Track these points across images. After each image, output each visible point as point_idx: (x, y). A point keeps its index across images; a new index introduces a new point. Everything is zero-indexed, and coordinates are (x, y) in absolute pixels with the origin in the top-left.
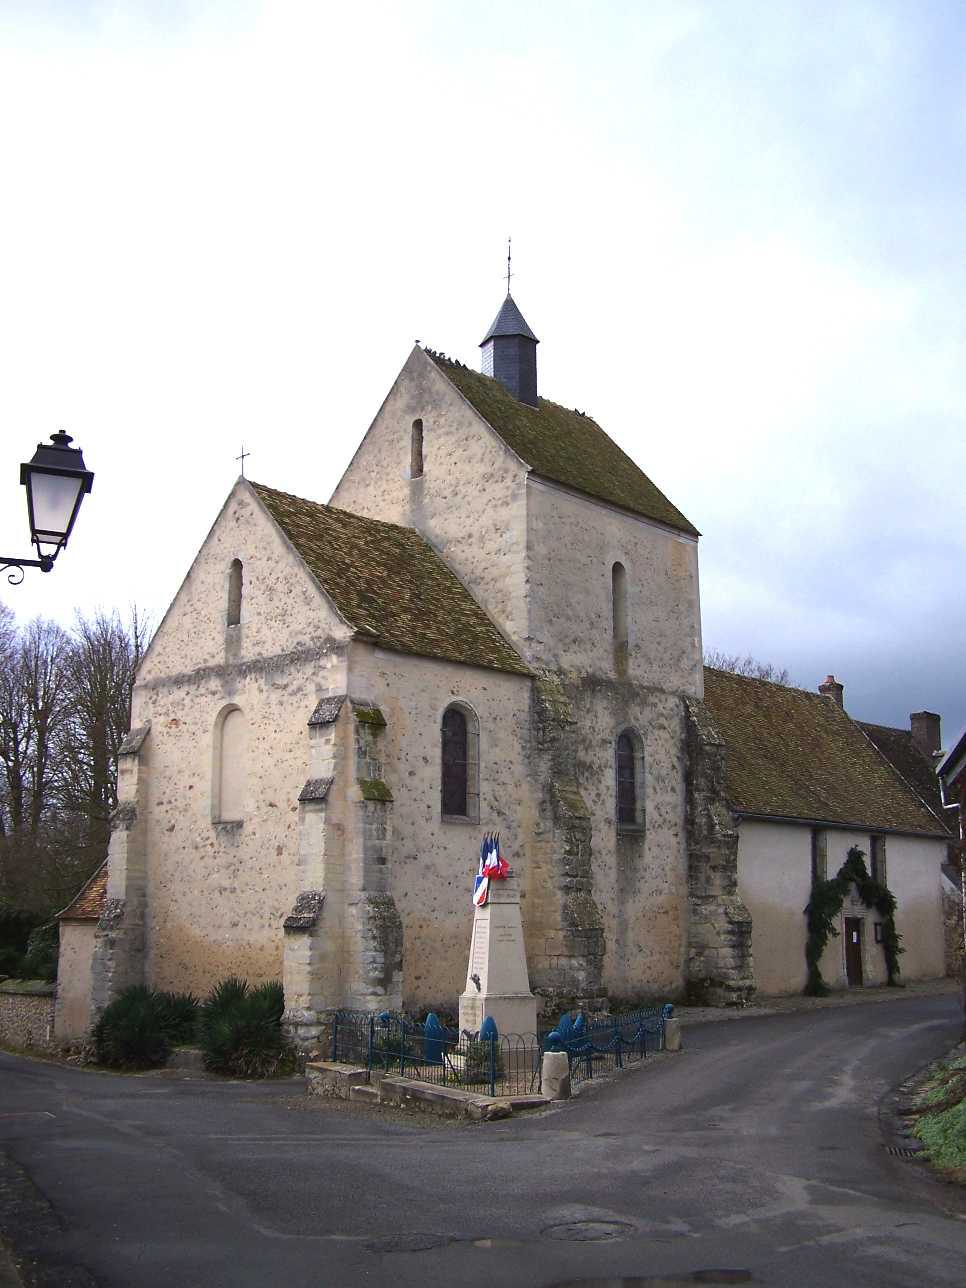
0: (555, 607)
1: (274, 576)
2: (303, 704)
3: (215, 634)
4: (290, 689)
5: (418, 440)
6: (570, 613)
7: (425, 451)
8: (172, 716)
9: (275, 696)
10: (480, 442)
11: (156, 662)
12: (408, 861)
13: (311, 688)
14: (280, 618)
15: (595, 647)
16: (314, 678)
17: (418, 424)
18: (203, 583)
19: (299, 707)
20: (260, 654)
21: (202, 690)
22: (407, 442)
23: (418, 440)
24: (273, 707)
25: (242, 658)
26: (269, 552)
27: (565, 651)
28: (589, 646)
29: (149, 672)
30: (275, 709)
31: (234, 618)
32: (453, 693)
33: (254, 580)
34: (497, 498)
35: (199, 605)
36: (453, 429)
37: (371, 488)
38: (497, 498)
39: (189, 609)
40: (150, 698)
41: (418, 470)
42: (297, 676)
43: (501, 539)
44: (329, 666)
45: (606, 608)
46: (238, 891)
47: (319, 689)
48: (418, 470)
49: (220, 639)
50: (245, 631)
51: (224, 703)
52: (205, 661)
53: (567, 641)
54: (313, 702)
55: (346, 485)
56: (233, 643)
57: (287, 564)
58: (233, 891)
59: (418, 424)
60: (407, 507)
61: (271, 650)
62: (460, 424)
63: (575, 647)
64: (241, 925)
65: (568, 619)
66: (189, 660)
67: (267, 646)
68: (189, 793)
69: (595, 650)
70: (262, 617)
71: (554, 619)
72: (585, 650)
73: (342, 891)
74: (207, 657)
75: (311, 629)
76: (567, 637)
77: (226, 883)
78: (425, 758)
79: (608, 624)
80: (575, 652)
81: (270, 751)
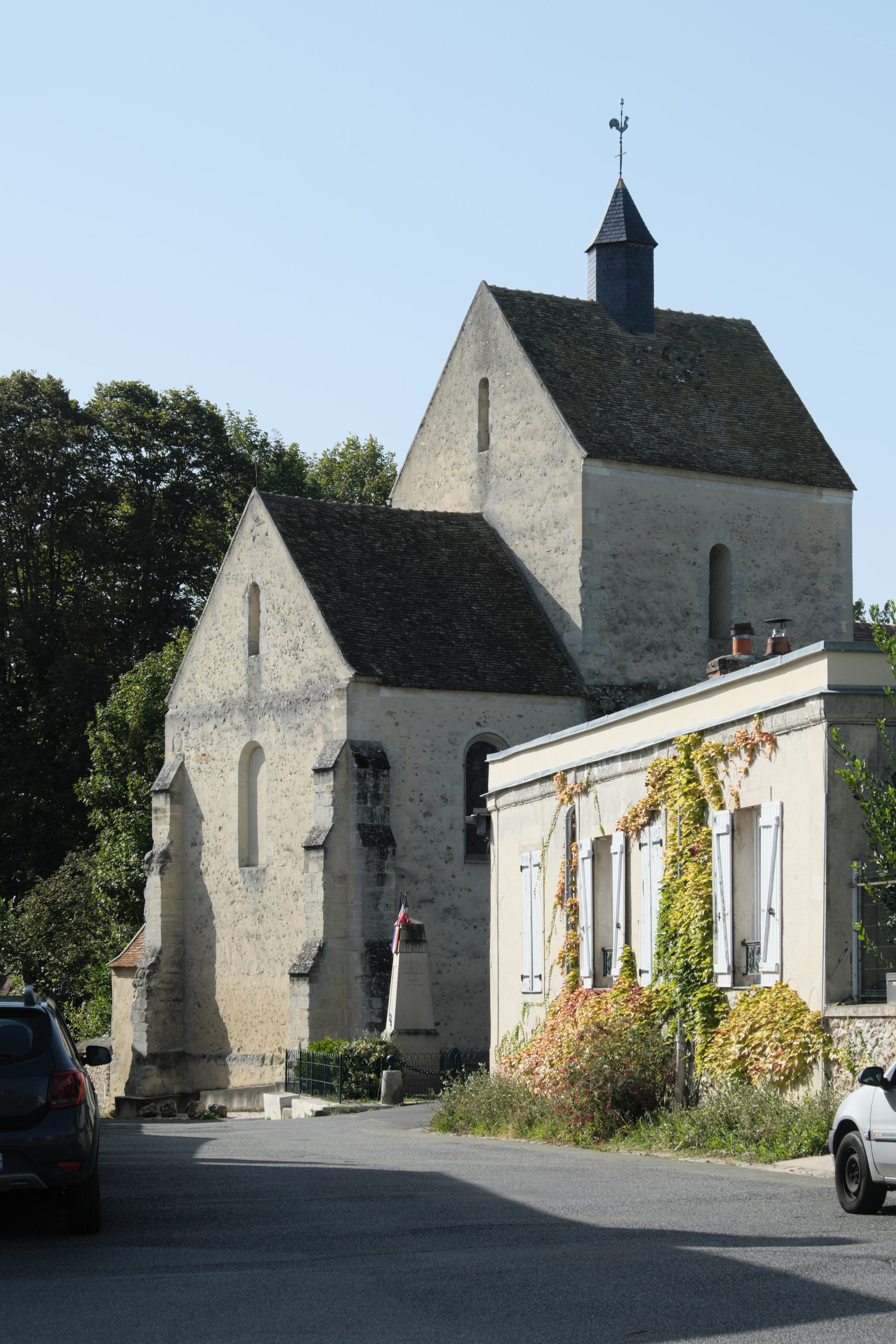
0: (621, 611)
1: (286, 607)
2: (312, 746)
3: (238, 663)
4: (302, 729)
5: (484, 404)
6: (643, 615)
7: (491, 420)
8: (202, 750)
9: (290, 736)
10: (542, 414)
11: (187, 688)
12: (423, 905)
13: (318, 730)
14: (293, 652)
15: (680, 651)
16: (321, 719)
17: (484, 383)
18: (226, 605)
19: (309, 749)
20: (277, 689)
21: (228, 724)
22: (474, 405)
23: (484, 404)
24: (288, 746)
25: (263, 692)
26: (283, 579)
27: (634, 661)
28: (671, 652)
29: (181, 700)
30: (290, 749)
31: (254, 649)
32: (478, 724)
33: (270, 607)
34: (557, 485)
35: (222, 630)
36: (517, 396)
37: (441, 458)
38: (557, 485)
39: (215, 634)
40: (183, 729)
41: (484, 443)
42: (307, 717)
43: (558, 536)
44: (332, 708)
45: (700, 605)
46: (263, 938)
47: (326, 730)
48: (484, 443)
49: (243, 669)
50: (264, 663)
51: (245, 741)
52: (231, 693)
53: (638, 649)
54: (320, 745)
55: (417, 452)
56: (253, 676)
57: (298, 594)
58: (258, 937)
59: (484, 383)
60: (475, 486)
61: (287, 685)
62: (524, 390)
63: (650, 656)
64: (265, 973)
65: (640, 622)
66: (216, 691)
67: (284, 680)
68: (220, 835)
69: (679, 655)
70: (278, 650)
71: (620, 626)
72: (666, 658)
73: (346, 937)
74: (232, 688)
75: (318, 668)
76: (639, 644)
77: (252, 929)
78: (443, 797)
79: (703, 623)
80: (650, 661)
81: (288, 794)
